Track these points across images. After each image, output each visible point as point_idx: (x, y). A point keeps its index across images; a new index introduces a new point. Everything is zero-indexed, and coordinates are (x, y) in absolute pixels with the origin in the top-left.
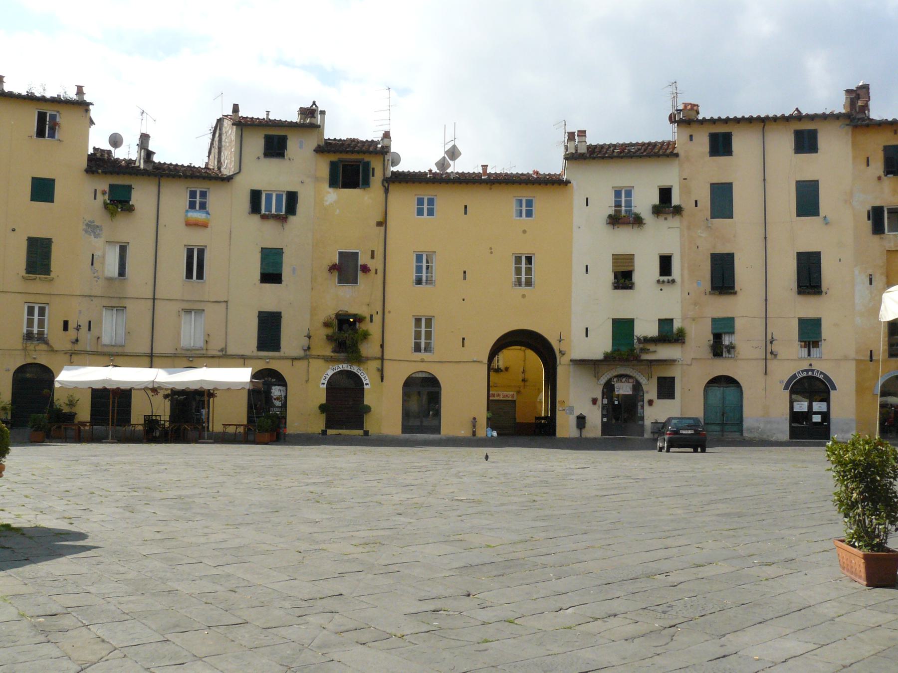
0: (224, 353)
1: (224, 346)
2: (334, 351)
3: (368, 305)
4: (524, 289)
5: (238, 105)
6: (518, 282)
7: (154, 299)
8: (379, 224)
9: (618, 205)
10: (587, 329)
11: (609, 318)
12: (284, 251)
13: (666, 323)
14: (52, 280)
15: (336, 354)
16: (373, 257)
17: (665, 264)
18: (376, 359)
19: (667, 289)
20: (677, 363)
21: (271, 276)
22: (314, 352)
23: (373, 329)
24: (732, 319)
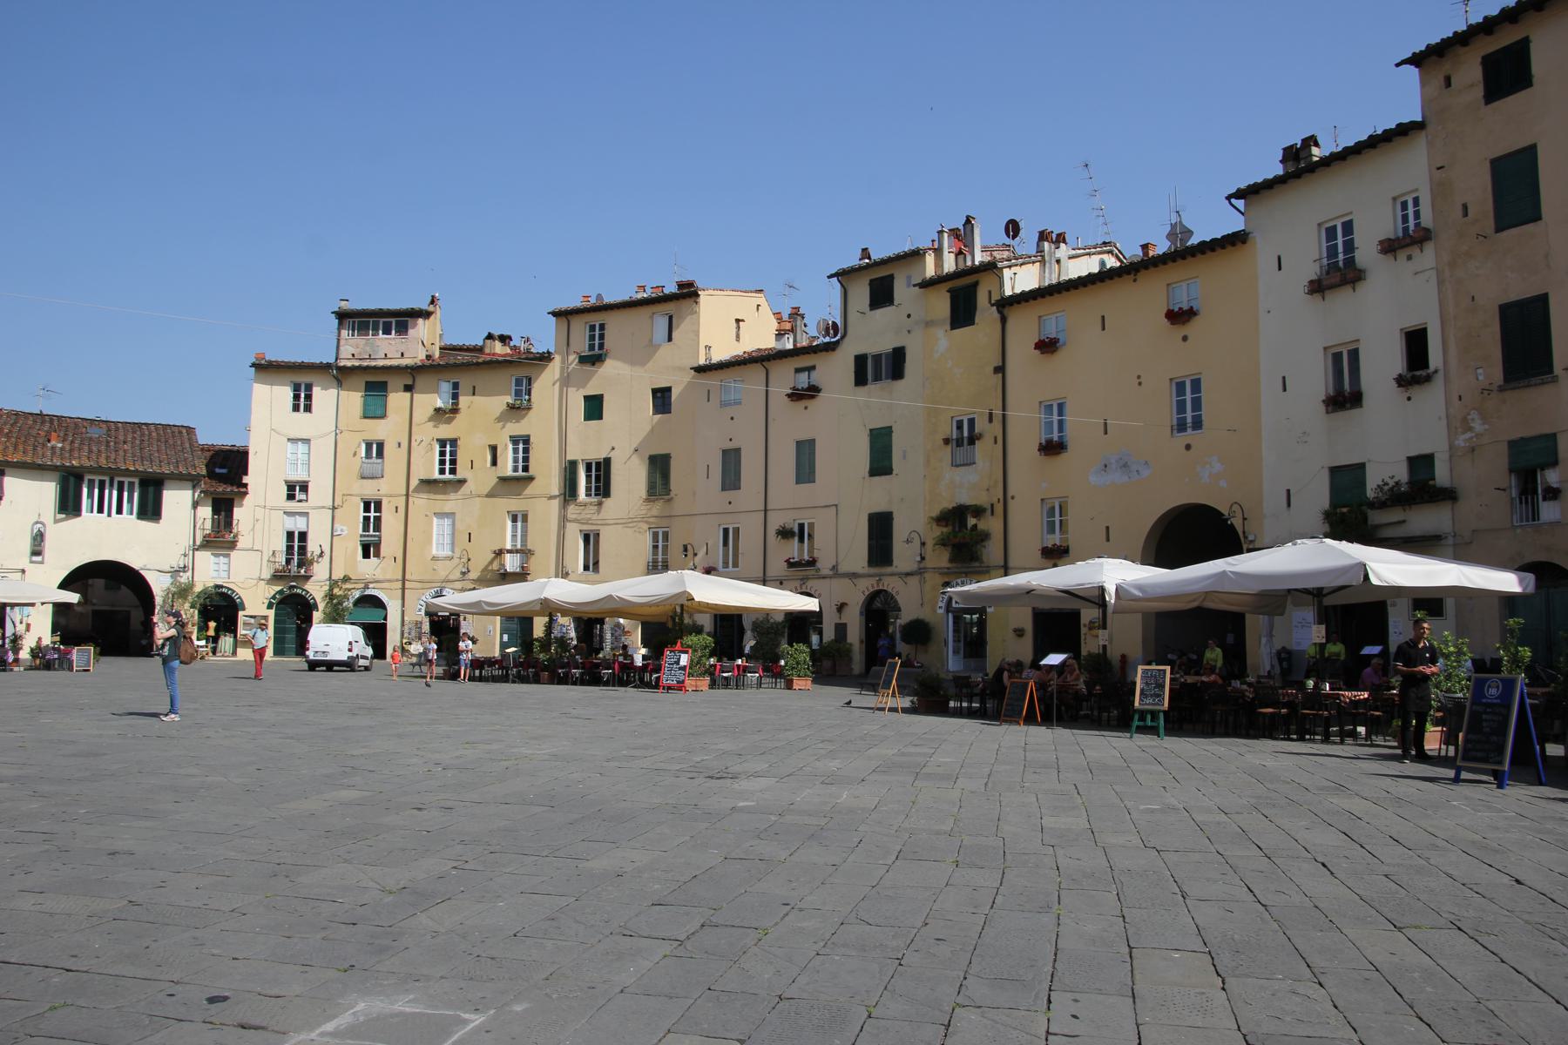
1: (835, 564)
2: (951, 560)
4: (1189, 435)
6: (1181, 426)
7: (766, 510)
9: (1332, 252)
11: (1323, 467)
12: (893, 429)
13: (1421, 464)
14: (669, 500)
15: (954, 565)
16: (991, 420)
17: (1416, 342)
20: (1443, 542)
21: (881, 464)
22: (928, 563)
23: (992, 524)
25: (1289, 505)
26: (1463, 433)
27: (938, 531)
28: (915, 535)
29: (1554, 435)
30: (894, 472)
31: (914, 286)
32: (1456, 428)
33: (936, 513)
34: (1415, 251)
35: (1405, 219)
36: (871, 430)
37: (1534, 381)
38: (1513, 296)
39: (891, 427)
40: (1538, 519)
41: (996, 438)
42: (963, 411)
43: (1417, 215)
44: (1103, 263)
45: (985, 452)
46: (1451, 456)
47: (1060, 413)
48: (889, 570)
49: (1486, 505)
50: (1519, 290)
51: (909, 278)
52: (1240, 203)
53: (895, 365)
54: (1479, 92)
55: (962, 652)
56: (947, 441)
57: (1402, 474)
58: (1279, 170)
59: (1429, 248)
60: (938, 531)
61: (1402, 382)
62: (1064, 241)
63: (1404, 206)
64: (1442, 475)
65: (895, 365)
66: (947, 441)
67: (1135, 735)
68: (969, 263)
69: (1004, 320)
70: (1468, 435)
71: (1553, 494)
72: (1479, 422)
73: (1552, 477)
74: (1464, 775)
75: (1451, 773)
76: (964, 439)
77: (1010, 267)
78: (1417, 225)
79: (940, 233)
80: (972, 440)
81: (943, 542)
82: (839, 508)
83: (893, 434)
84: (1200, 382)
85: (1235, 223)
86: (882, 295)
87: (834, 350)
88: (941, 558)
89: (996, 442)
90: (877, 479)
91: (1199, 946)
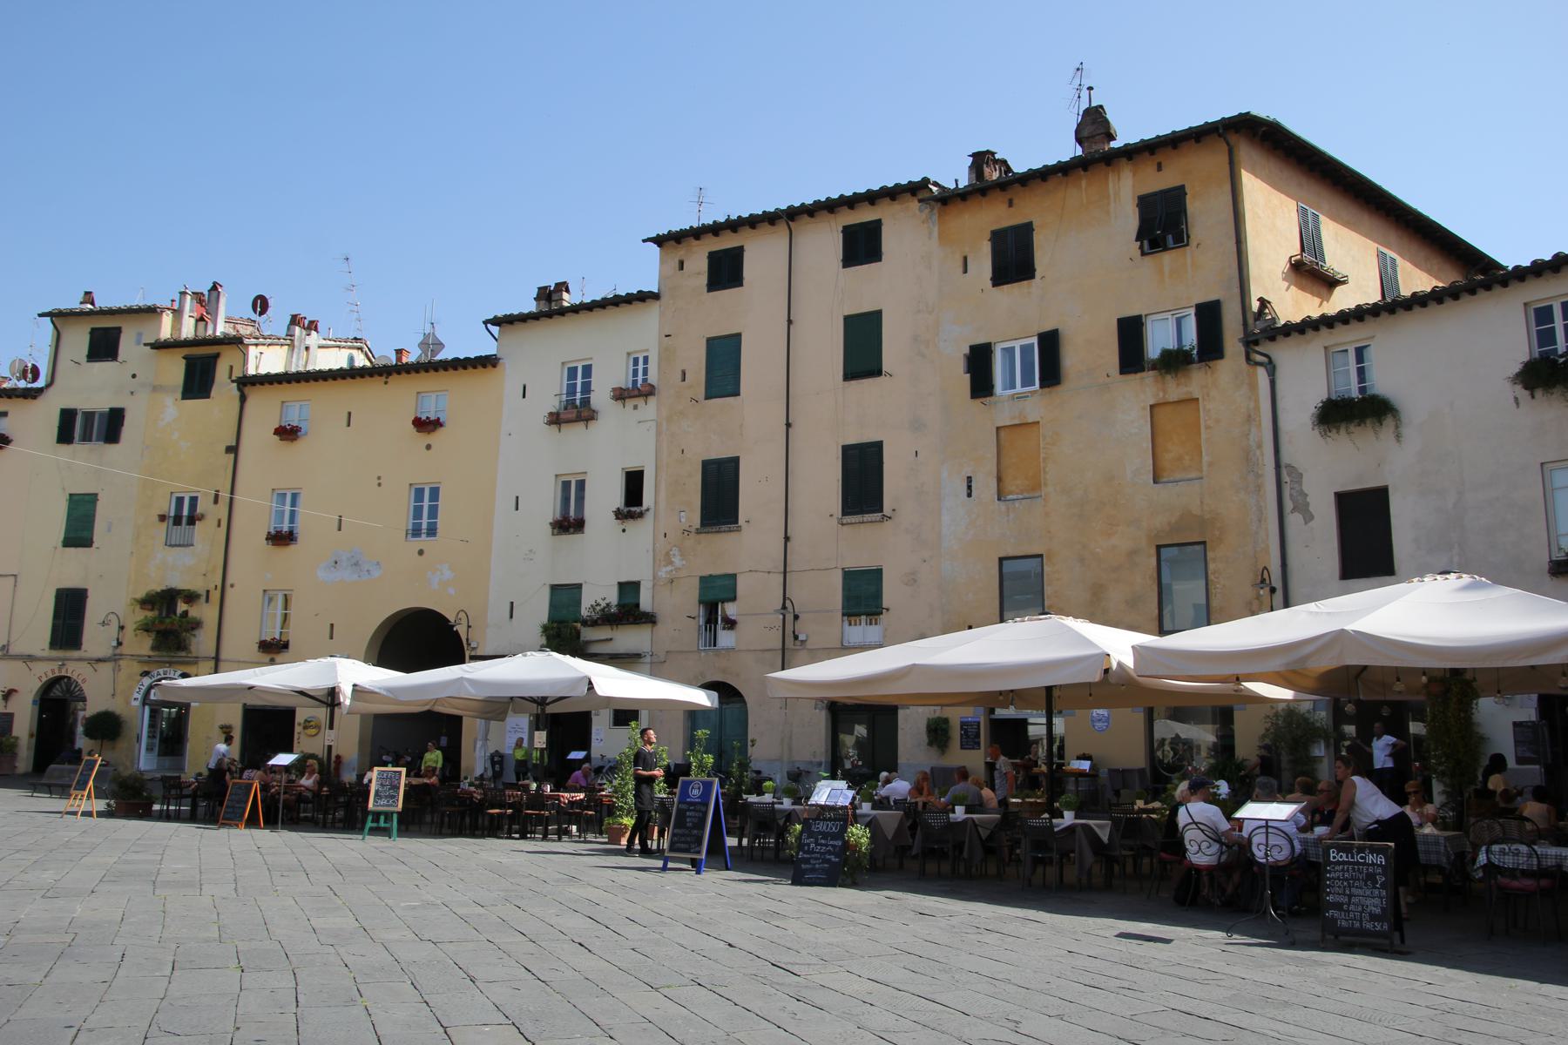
0: (5, 652)
1: (5, 643)
2: (153, 648)
3: (204, 575)
4: (423, 541)
5: (91, 293)
6: (416, 532)
8: (230, 449)
9: (571, 390)
10: (512, 603)
12: (99, 498)
13: (629, 589)
15: (156, 653)
16: (216, 501)
17: (634, 482)
18: (207, 658)
19: (630, 525)
20: (642, 660)
21: (79, 532)
22: (125, 650)
23: (205, 612)
24: (733, 577)
25: (511, 617)
26: (666, 566)
27: (142, 615)
28: (112, 617)
29: (736, 575)
30: (95, 545)
31: (145, 345)
32: (660, 560)
33: (141, 594)
34: (640, 402)
35: (635, 373)
36: (71, 495)
37: (724, 527)
38: (713, 456)
39: (96, 495)
40: (715, 646)
41: (219, 521)
42: (186, 489)
43: (645, 372)
44: (351, 359)
45: (205, 535)
46: (654, 586)
47: (294, 504)
48: (76, 654)
49: (679, 630)
50: (719, 451)
51: (140, 335)
52: (495, 330)
53: (111, 426)
54: (704, 280)
55: (156, 749)
56: (162, 518)
57: (612, 597)
58: (530, 306)
59: (652, 400)
60: (142, 615)
61: (619, 515)
62: (316, 330)
63: (636, 361)
64: (645, 603)
65: (111, 426)
66: (162, 518)
67: (367, 837)
68: (210, 332)
69: (243, 399)
70: (669, 568)
71: (731, 624)
72: (679, 557)
73: (731, 609)
74: (670, 865)
75: (660, 863)
76: (184, 516)
77: (256, 345)
78: (645, 380)
79: (183, 294)
80: (192, 520)
81: (146, 628)
82: (18, 580)
83: (98, 503)
84: (640, 585)
85: (487, 347)
86: (104, 346)
87: (35, 398)
88: (143, 645)
89: (219, 525)
90: (72, 550)
91: (503, 1020)
